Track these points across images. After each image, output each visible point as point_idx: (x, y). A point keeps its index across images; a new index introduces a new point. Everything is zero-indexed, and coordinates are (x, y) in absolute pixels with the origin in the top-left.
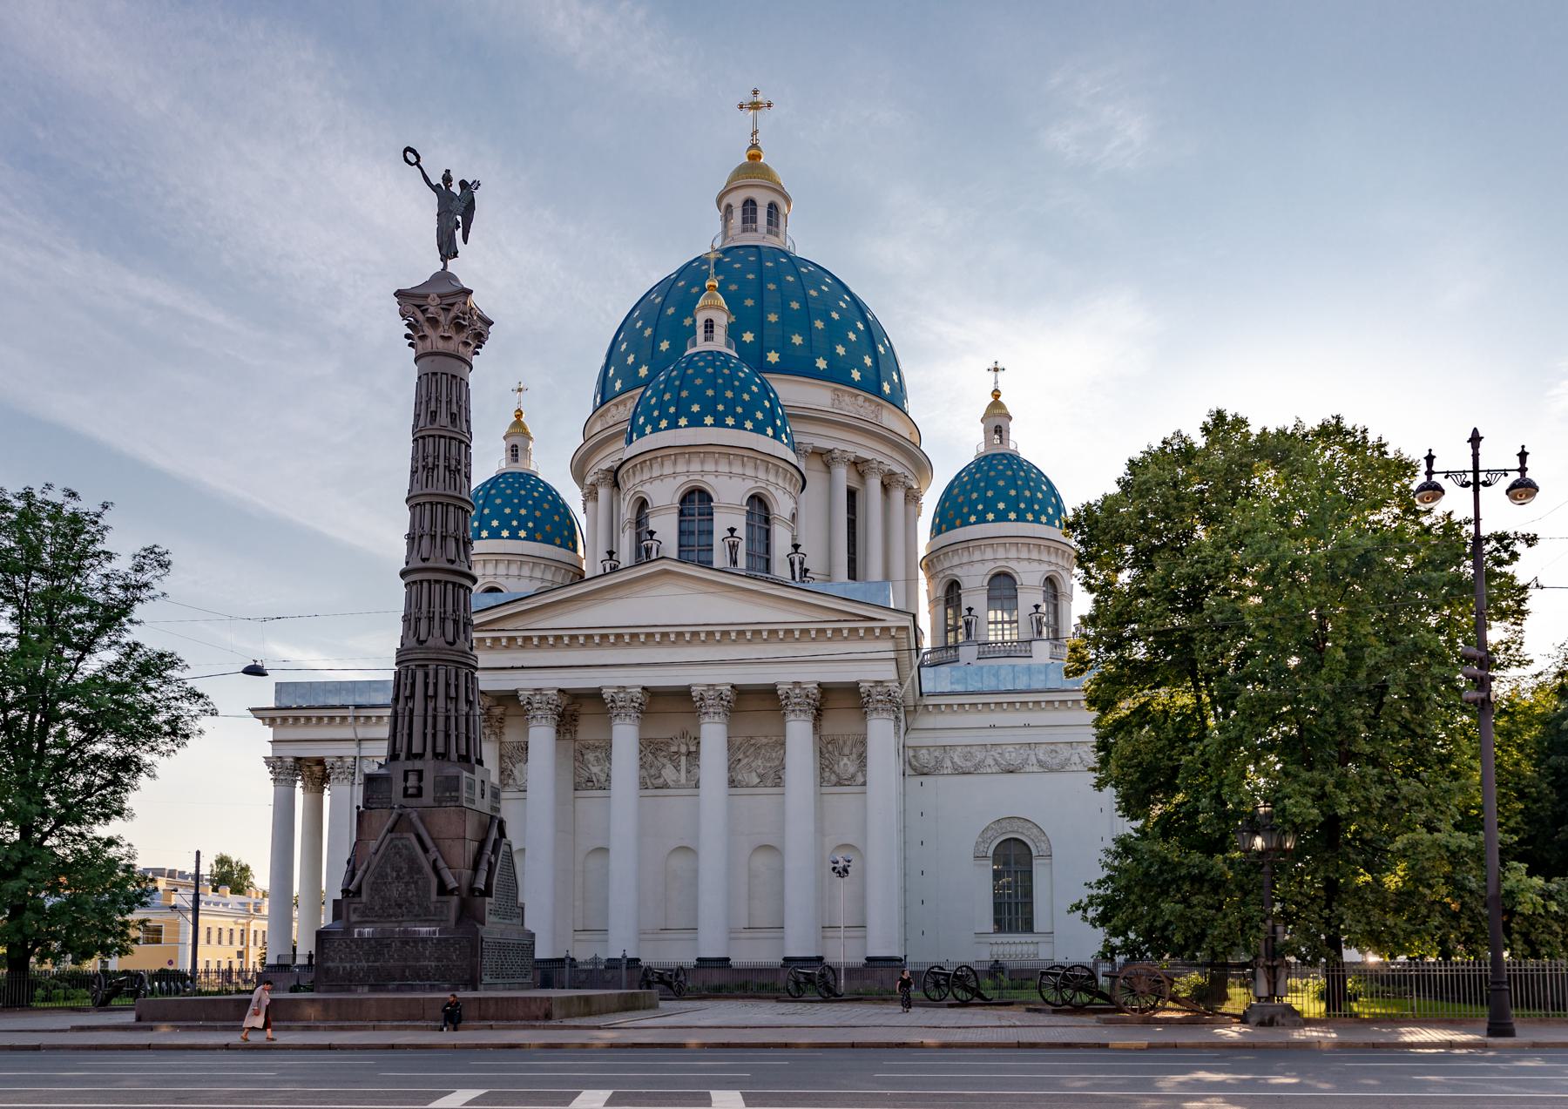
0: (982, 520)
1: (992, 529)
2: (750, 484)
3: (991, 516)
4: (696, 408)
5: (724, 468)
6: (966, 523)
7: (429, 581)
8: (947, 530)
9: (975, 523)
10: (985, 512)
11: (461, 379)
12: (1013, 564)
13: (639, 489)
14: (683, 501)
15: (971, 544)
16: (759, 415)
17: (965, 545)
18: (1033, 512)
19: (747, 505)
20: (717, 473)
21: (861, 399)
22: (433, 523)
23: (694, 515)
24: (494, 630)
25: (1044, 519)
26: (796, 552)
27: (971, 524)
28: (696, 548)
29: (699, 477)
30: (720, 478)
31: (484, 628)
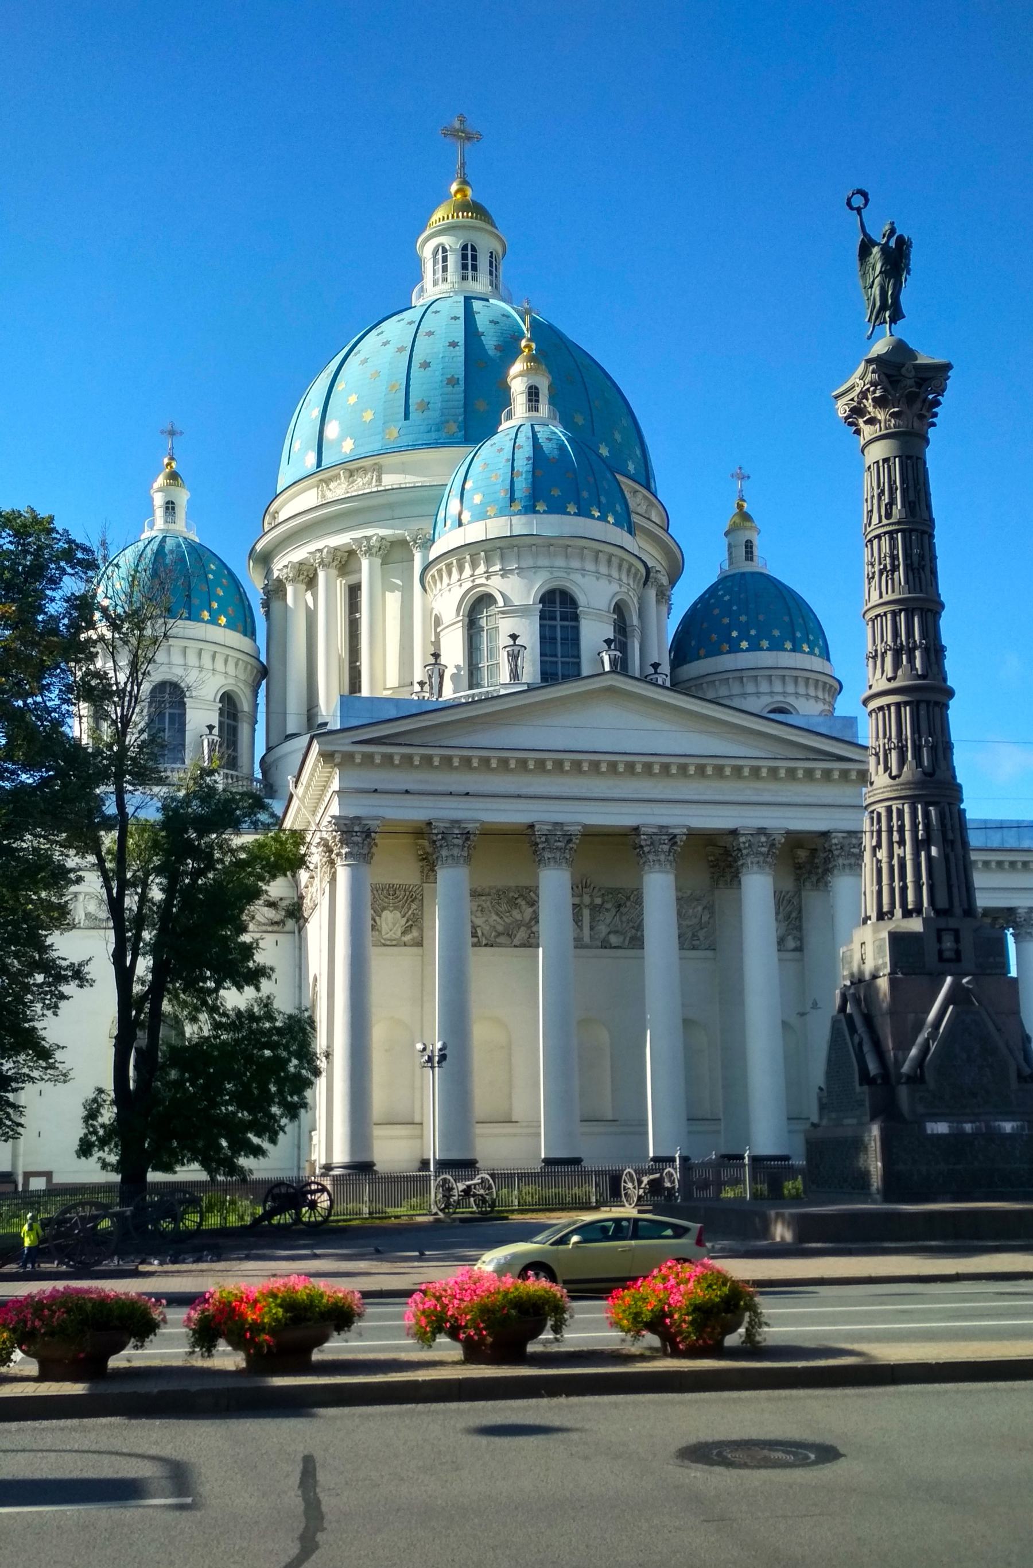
0: (755, 647)
1: (766, 658)
2: (615, 587)
3: (765, 644)
4: (556, 492)
5: (590, 566)
6: (735, 649)
7: (928, 703)
8: (706, 657)
9: (747, 650)
10: (759, 638)
11: (918, 458)
12: (791, 700)
13: (483, 581)
14: (542, 600)
15: (745, 674)
16: (618, 508)
17: (738, 674)
18: (808, 642)
19: (614, 612)
20: (583, 571)
21: (640, 496)
22: (896, 634)
23: (555, 619)
24: (400, 744)
25: (817, 651)
26: (656, 673)
27: (742, 651)
28: (560, 659)
29: (565, 575)
30: (587, 577)
31: (339, 742)
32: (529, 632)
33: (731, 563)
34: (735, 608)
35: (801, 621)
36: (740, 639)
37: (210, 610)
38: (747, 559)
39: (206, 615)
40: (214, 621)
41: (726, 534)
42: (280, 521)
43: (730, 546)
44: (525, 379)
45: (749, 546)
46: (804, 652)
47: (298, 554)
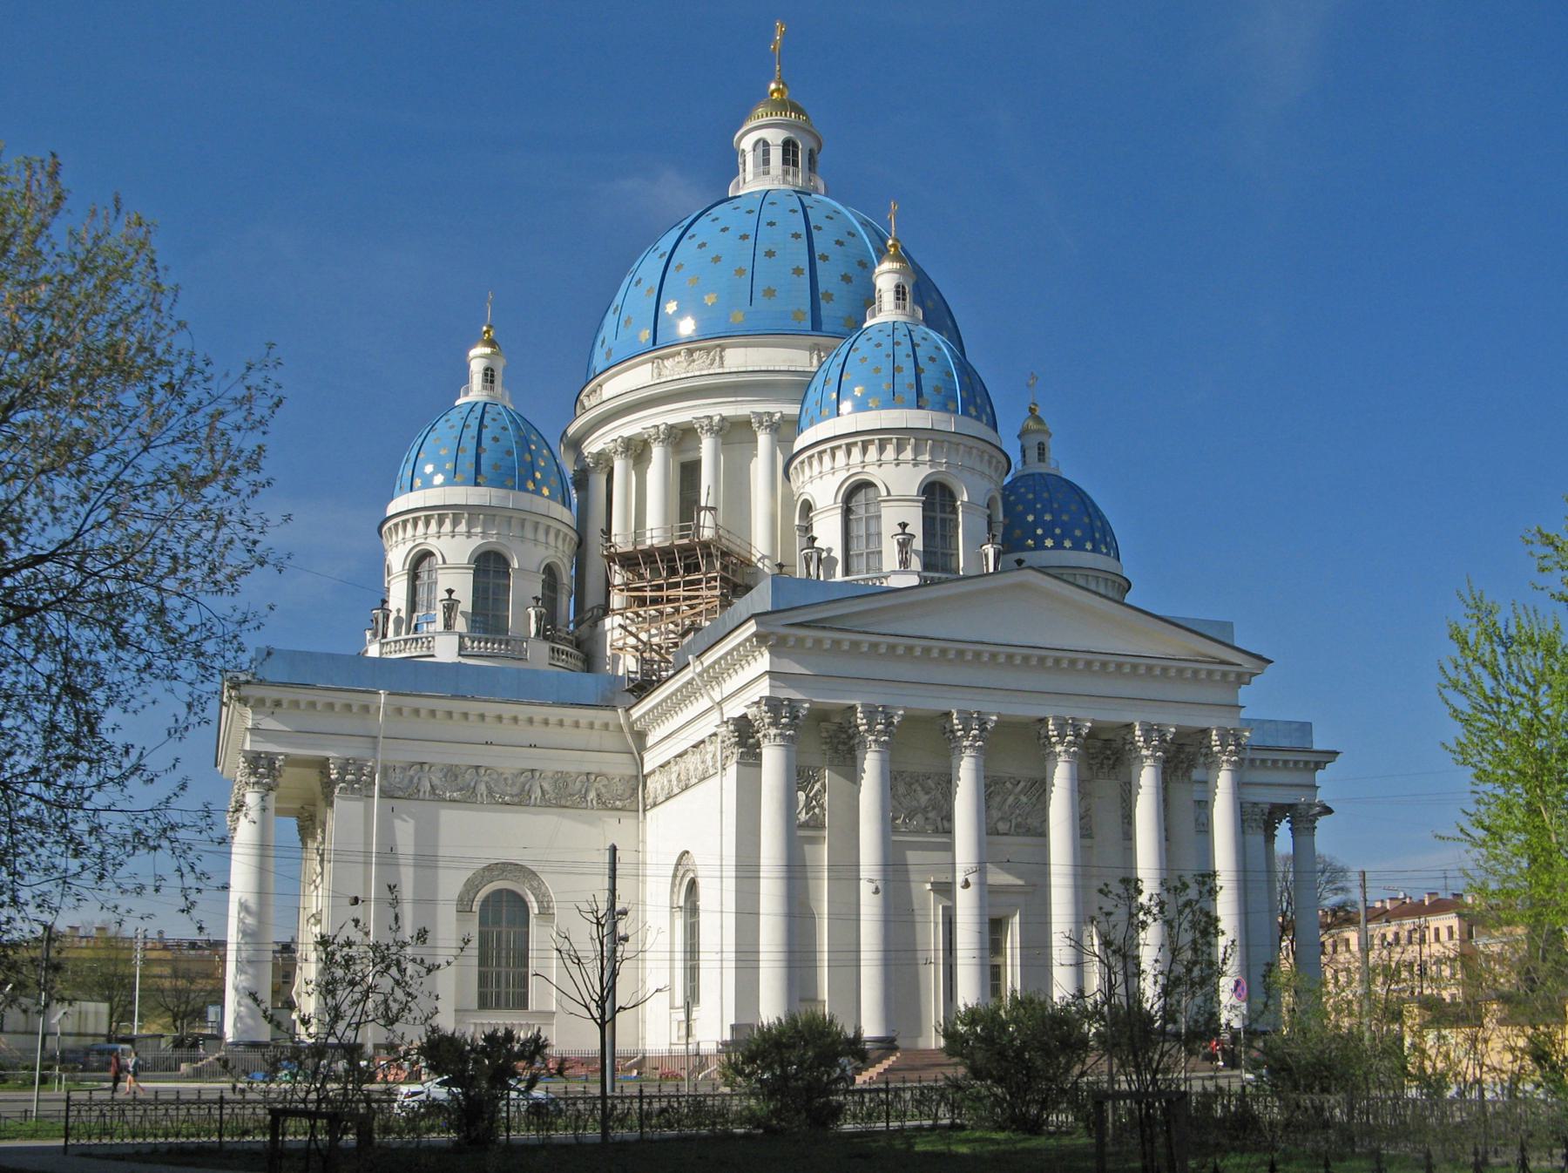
0: (1058, 546)
10: (1063, 536)
32: (914, 518)
33: (1024, 463)
34: (1039, 506)
35: (1099, 524)
36: (1044, 537)
37: (534, 480)
38: (1040, 460)
39: (531, 486)
40: (538, 492)
41: (1019, 437)
42: (604, 398)
43: (1022, 446)
44: (896, 276)
45: (1042, 449)
46: (1101, 553)
47: (631, 426)
